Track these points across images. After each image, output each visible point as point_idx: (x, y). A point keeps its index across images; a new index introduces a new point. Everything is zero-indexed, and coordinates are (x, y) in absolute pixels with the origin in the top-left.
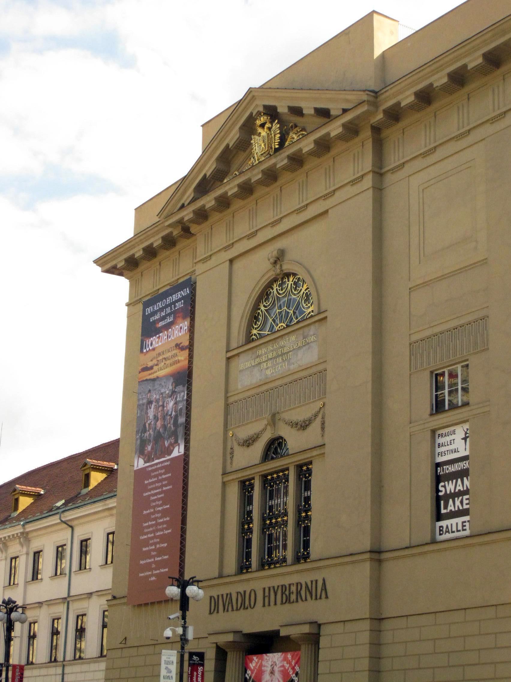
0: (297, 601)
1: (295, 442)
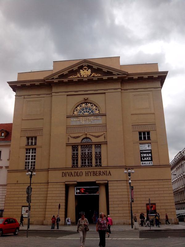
0: (99, 175)
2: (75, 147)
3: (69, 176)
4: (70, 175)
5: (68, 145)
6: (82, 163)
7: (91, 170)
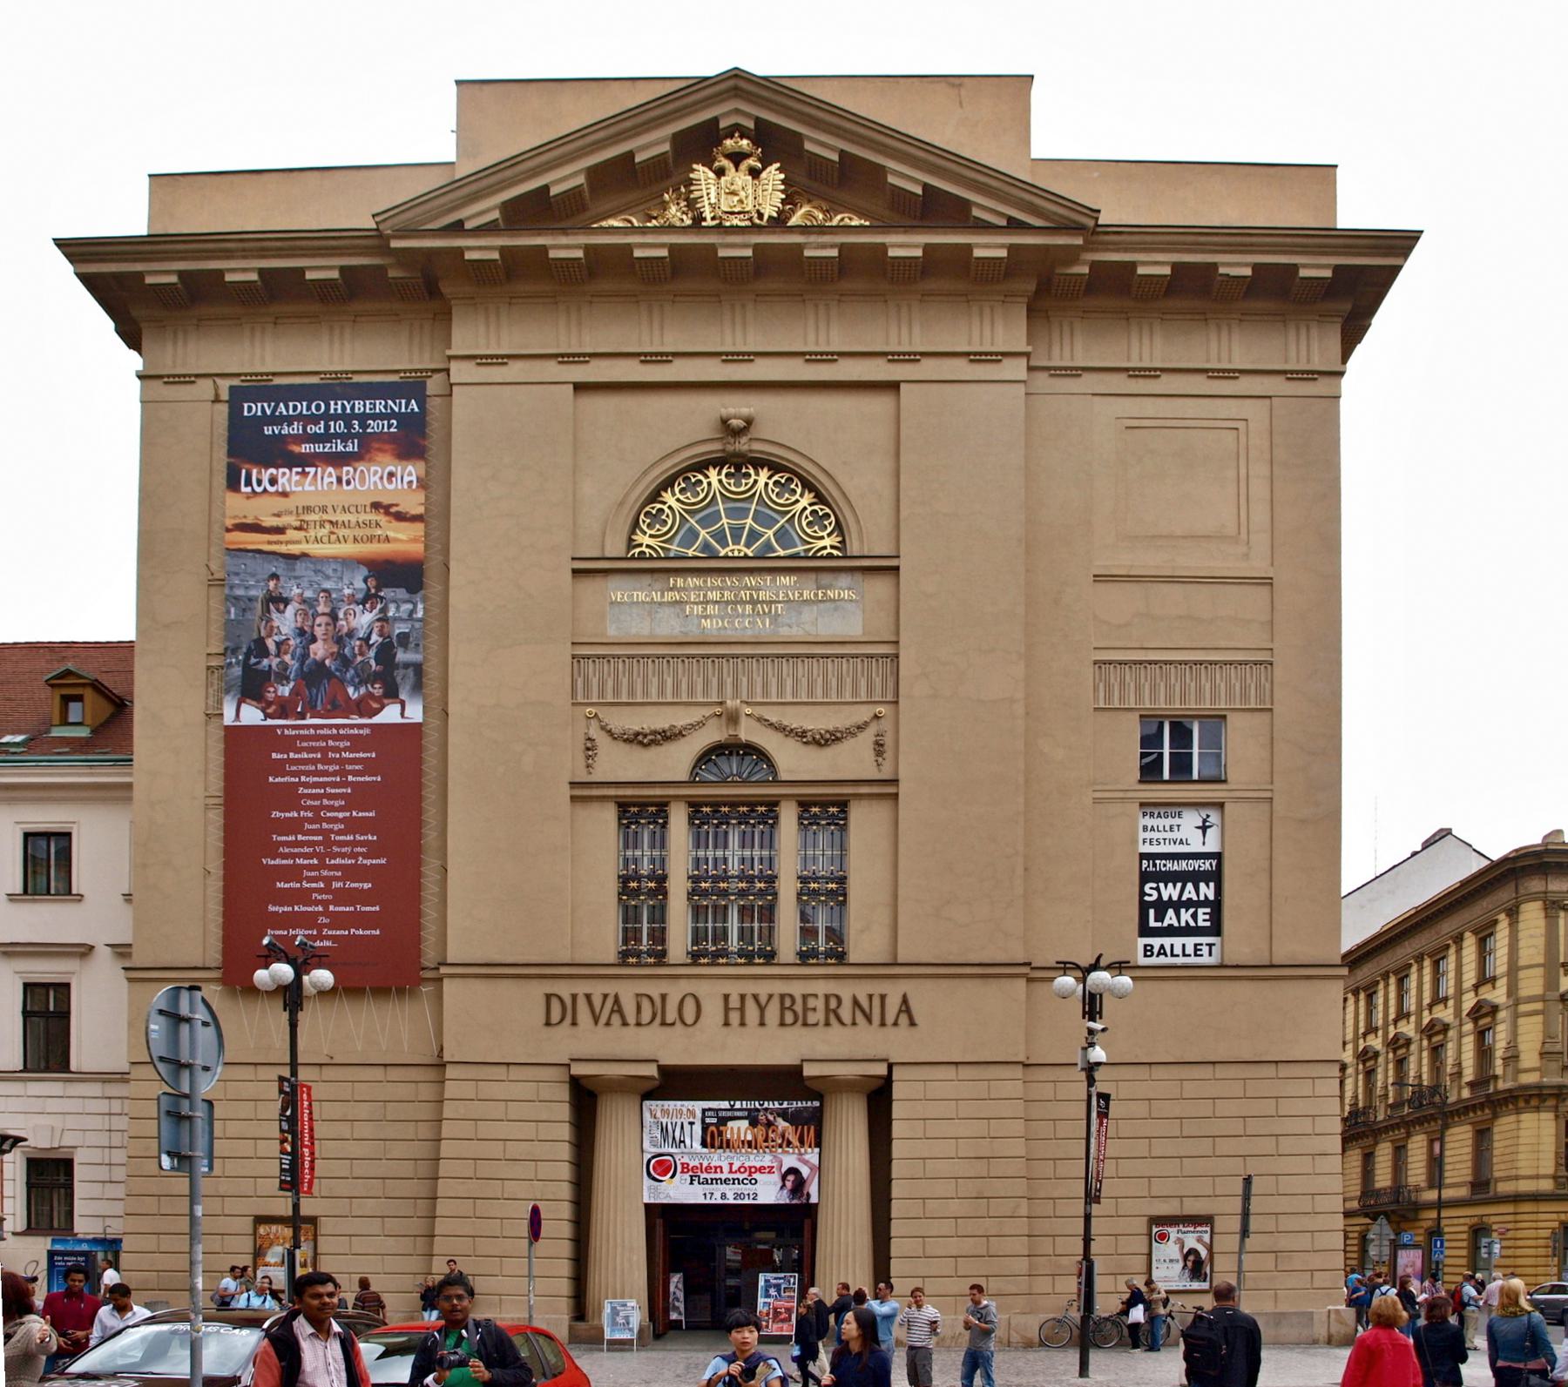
2: (640, 812)
3: (596, 1022)
4: (603, 1020)
5: (583, 793)
6: (698, 936)
7: (763, 989)
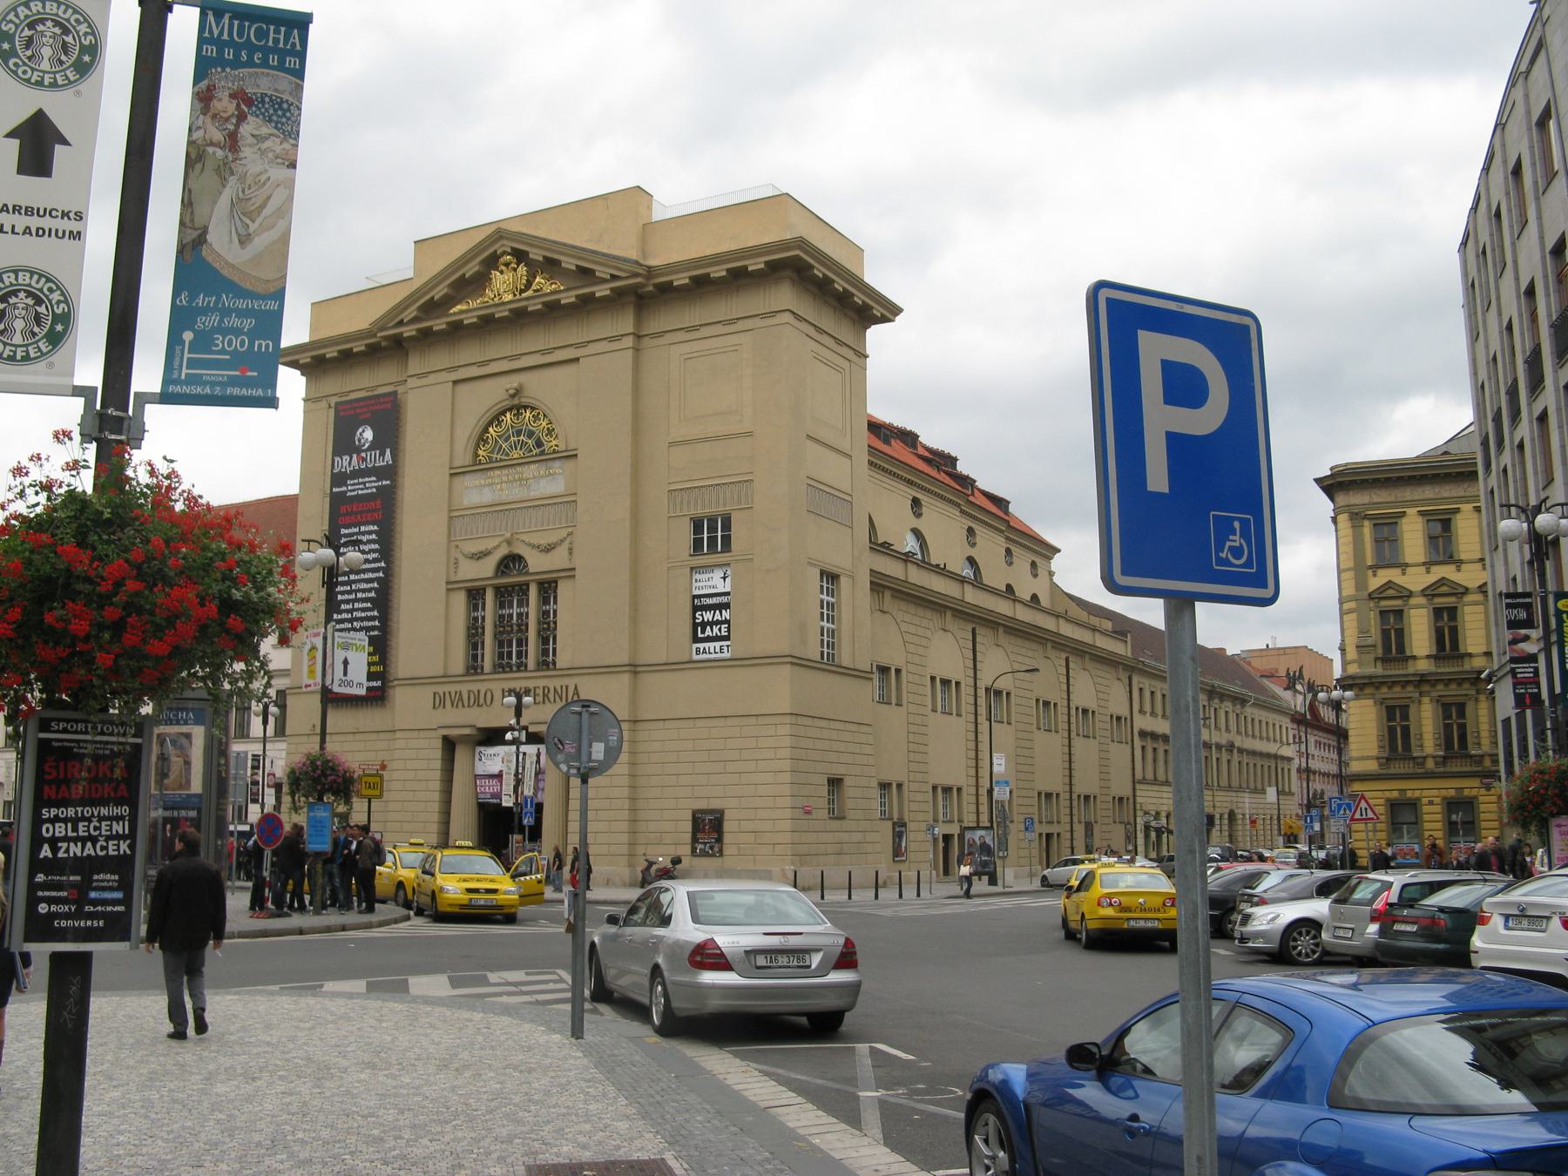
1: (538, 563)
5: (451, 586)
